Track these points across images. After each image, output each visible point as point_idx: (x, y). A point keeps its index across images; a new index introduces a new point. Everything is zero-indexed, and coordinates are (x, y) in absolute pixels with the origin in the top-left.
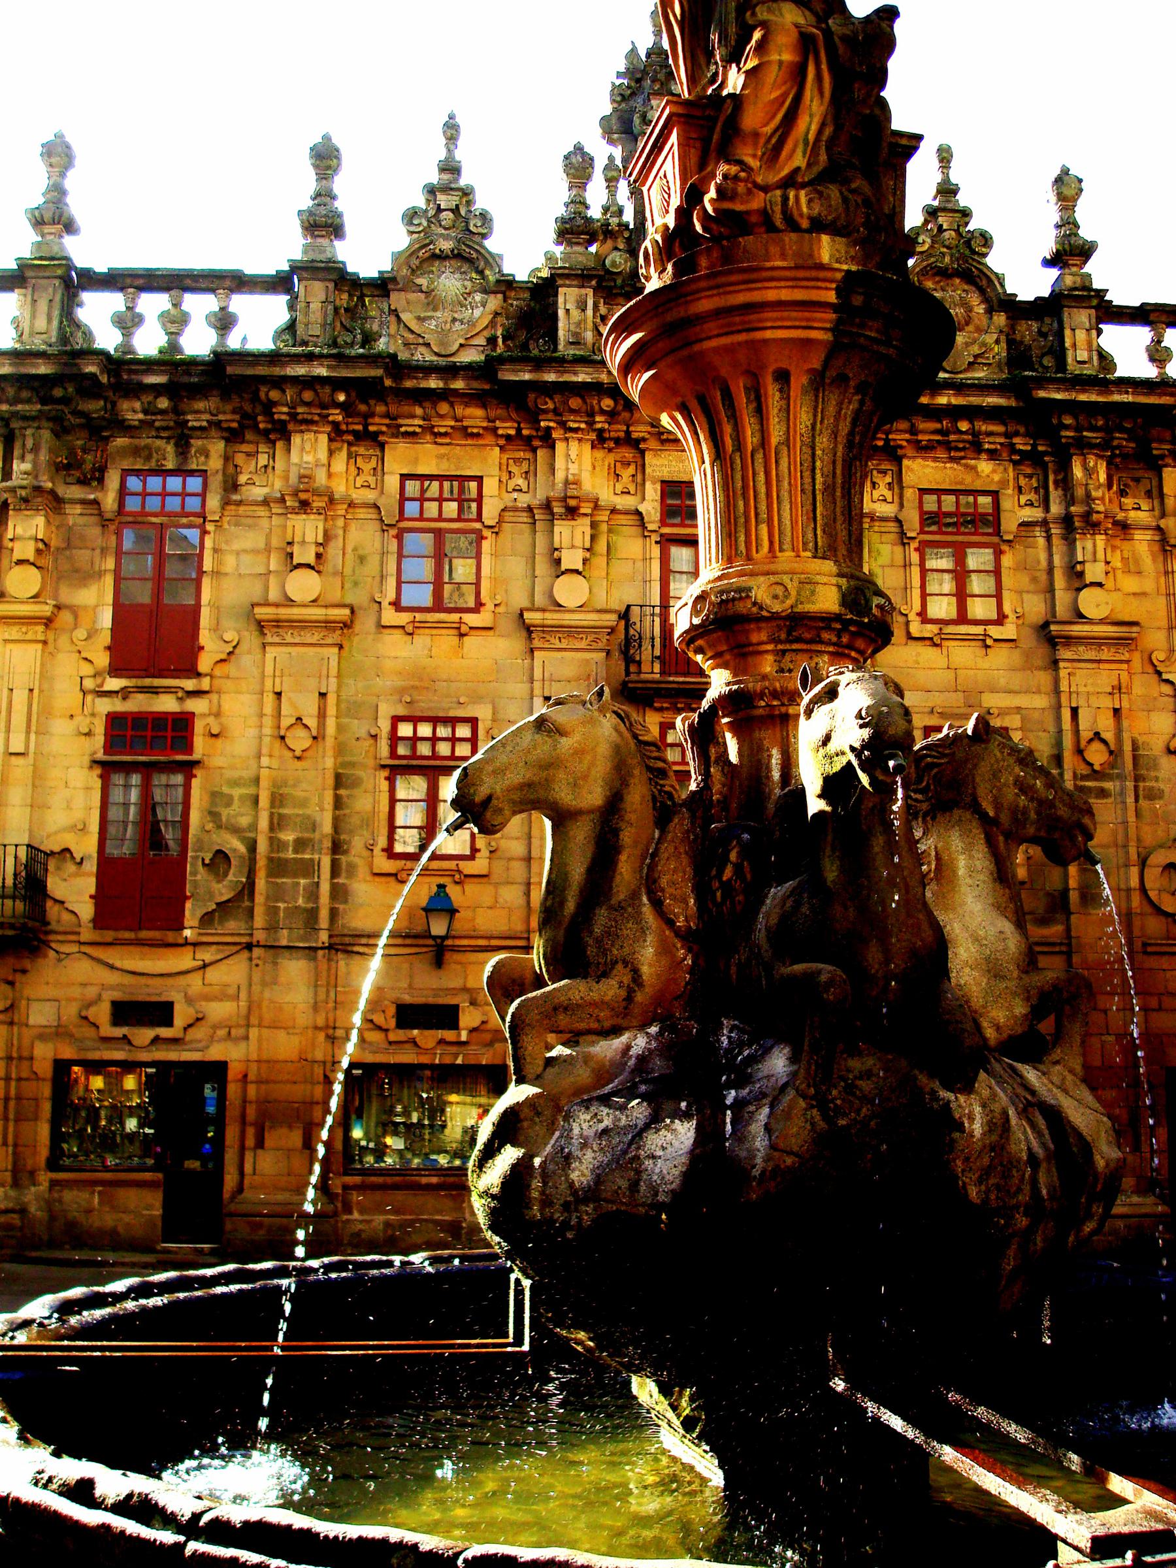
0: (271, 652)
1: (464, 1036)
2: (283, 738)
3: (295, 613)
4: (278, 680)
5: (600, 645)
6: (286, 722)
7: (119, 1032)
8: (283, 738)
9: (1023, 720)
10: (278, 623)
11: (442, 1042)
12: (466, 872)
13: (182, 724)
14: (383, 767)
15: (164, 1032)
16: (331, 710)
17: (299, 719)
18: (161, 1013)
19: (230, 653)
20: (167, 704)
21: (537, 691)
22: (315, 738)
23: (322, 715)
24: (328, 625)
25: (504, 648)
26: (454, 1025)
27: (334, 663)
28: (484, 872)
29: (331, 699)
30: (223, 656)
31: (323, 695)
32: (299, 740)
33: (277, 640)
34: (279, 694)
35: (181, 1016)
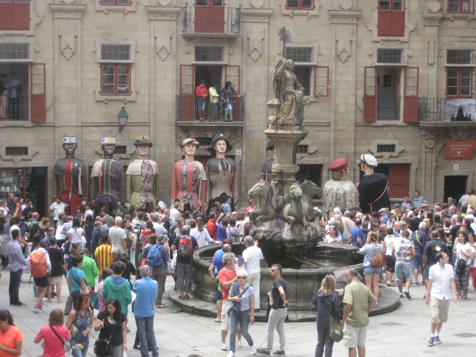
0: (56, 22)
1: (129, 157)
2: (62, 53)
3: (66, 7)
4: (60, 32)
5: (174, 19)
6: (63, 48)
7: (10, 157)
8: (62, 53)
9: (319, 45)
10: (59, 11)
11: (121, 158)
12: (128, 100)
13: (25, 47)
14: (99, 63)
15: (25, 157)
16: (79, 42)
17: (68, 46)
18: (23, 151)
19: (41, 21)
20: (20, 40)
21: (152, 35)
22: (73, 53)
23: (76, 44)
24: (77, 11)
25: (139, 18)
26: (124, 152)
27: (79, 25)
28: (133, 100)
29: (79, 38)
30: (39, 22)
31: (76, 37)
32: (68, 53)
33: (59, 16)
34: (60, 37)
35: (30, 152)
